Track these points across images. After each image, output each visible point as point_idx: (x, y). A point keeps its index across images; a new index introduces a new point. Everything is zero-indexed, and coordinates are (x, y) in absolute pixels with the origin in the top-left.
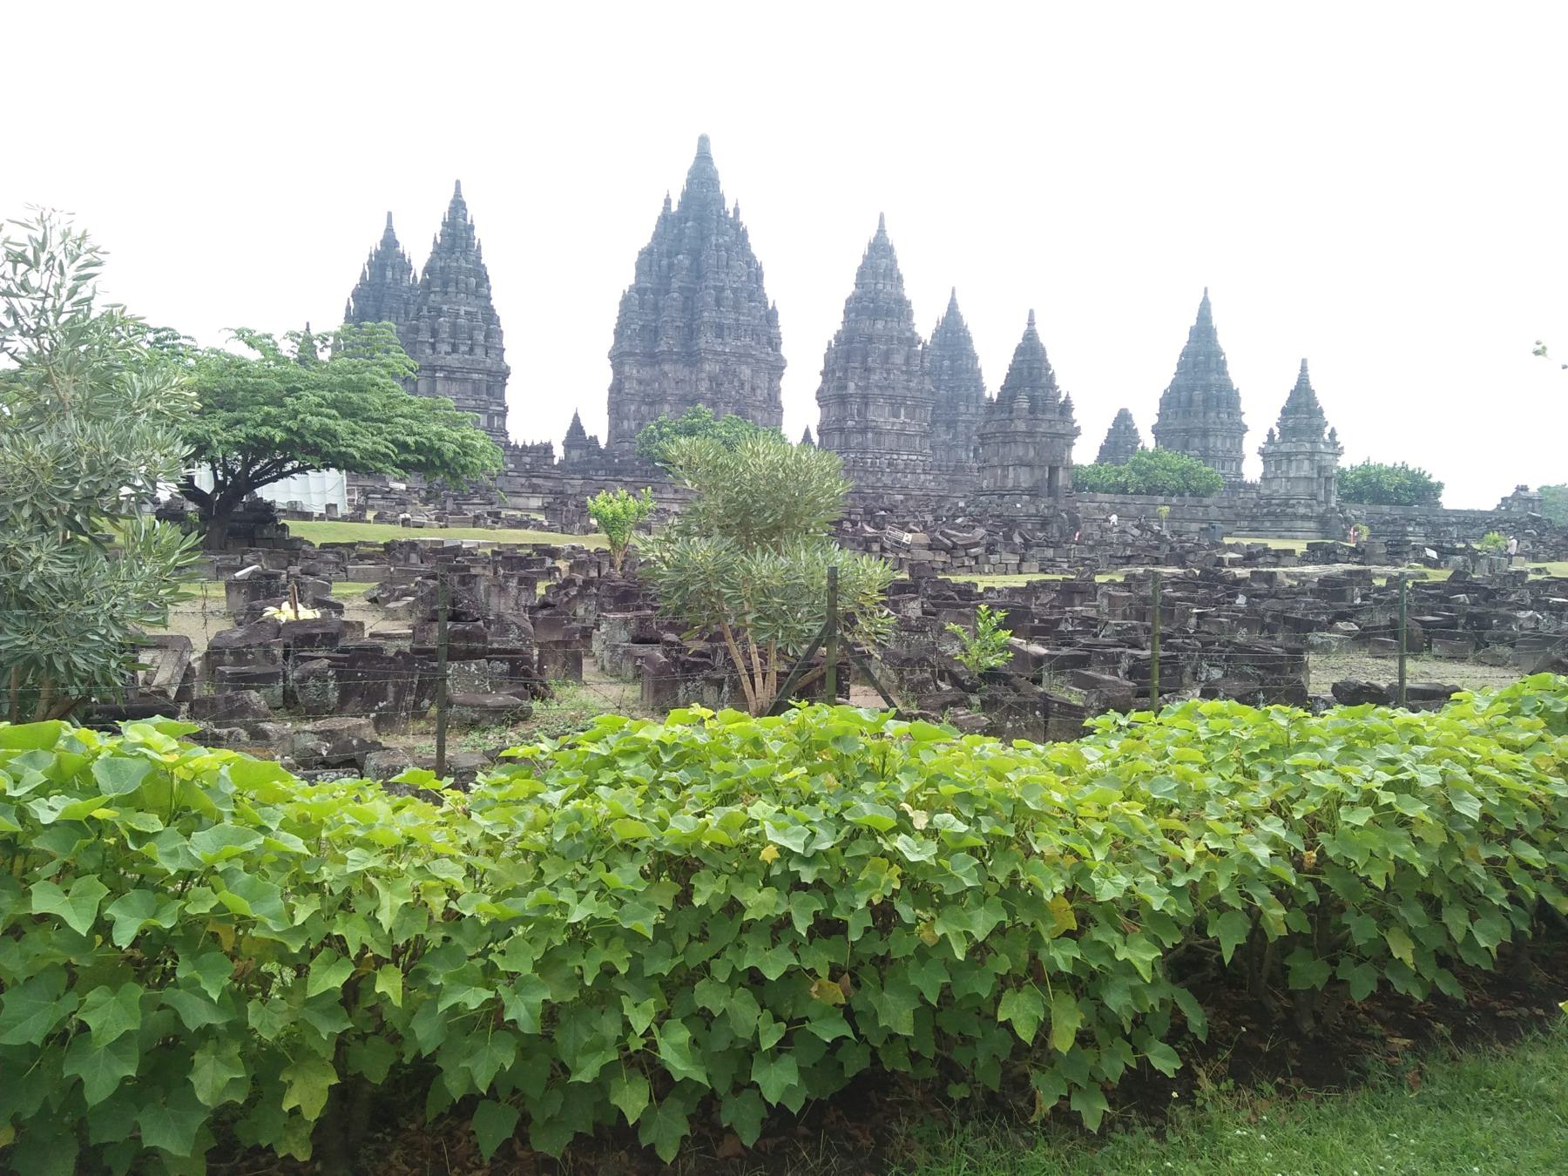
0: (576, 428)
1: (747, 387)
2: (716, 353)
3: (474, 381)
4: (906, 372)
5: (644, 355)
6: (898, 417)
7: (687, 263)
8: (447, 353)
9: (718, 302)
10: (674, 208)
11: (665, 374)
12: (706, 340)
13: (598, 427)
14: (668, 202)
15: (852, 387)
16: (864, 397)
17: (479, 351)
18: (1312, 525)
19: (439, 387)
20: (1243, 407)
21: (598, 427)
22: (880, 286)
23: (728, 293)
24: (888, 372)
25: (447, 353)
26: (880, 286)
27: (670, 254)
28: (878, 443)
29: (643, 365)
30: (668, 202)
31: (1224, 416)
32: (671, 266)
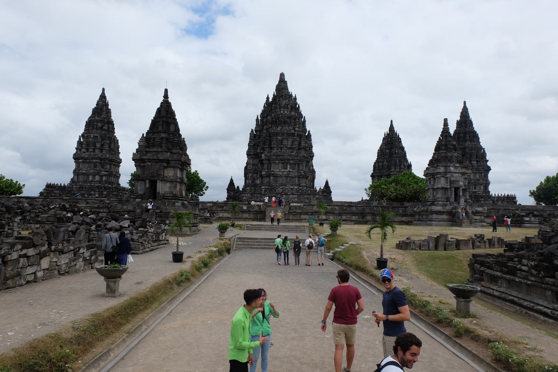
0: (232, 183)
3: (94, 163)
4: (291, 148)
5: (255, 155)
6: (286, 169)
8: (84, 152)
10: (270, 100)
13: (240, 183)
14: (268, 98)
16: (269, 160)
17: (97, 151)
18: (445, 217)
19: (81, 166)
20: (487, 158)
21: (240, 183)
22: (282, 112)
24: (281, 148)
25: (84, 152)
26: (282, 112)
28: (276, 181)
30: (268, 98)
31: (474, 163)
32: (266, 121)
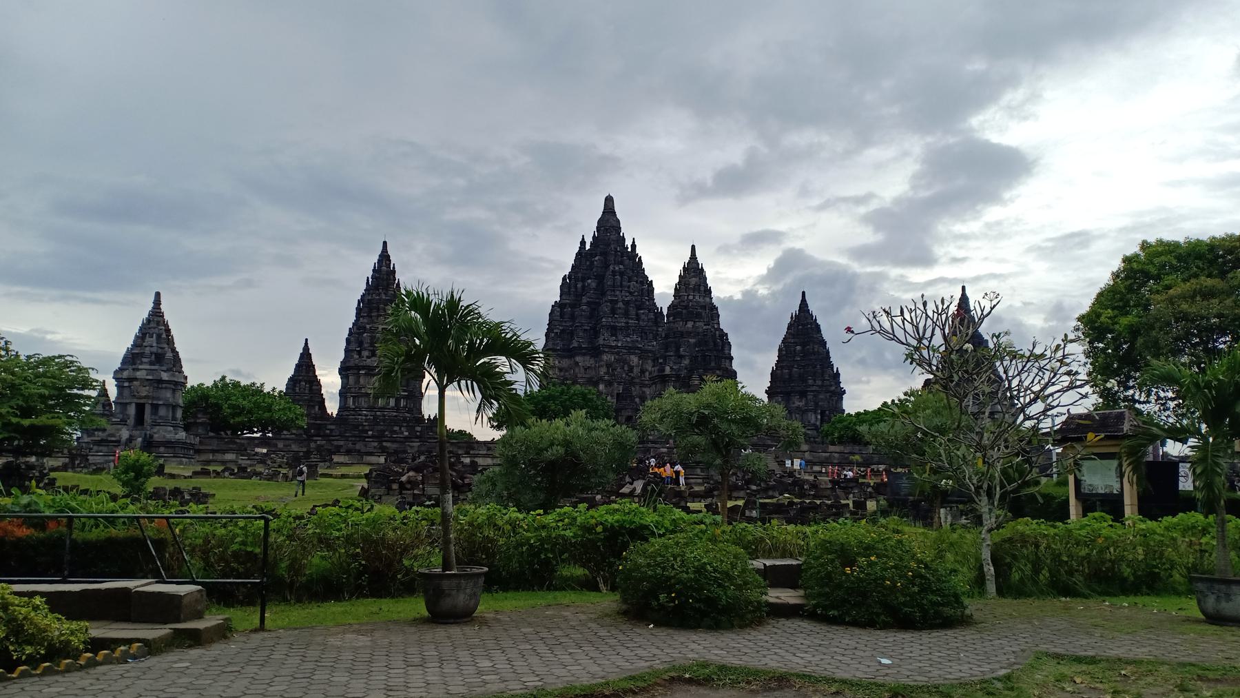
1: (636, 370)
2: (611, 347)
5: (564, 350)
7: (594, 285)
9: (613, 311)
10: (588, 247)
11: (577, 364)
12: (604, 338)
14: (583, 243)
15: (668, 370)
19: (362, 381)
23: (620, 305)
27: (584, 280)
29: (562, 357)
30: (583, 243)
32: (583, 287)
